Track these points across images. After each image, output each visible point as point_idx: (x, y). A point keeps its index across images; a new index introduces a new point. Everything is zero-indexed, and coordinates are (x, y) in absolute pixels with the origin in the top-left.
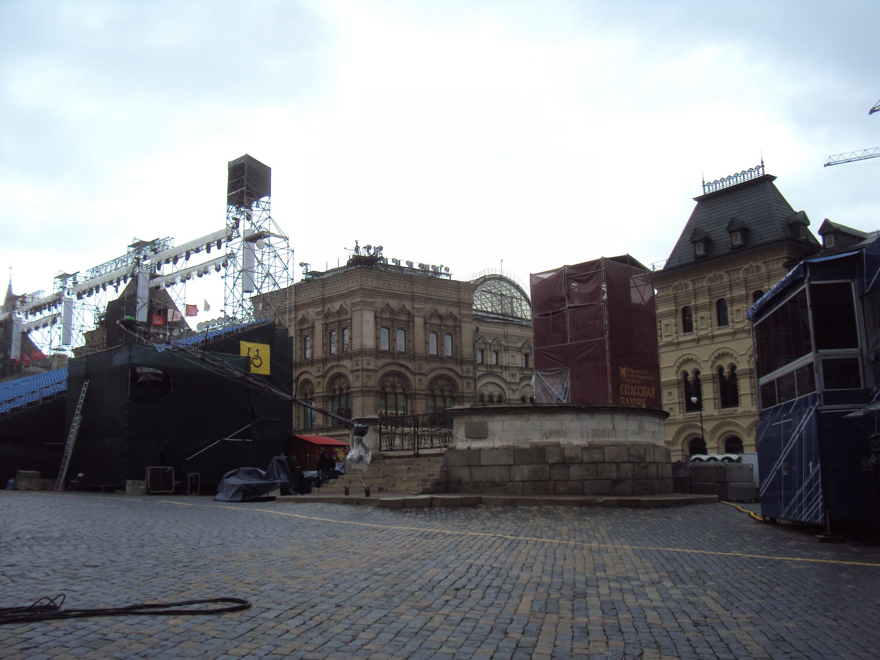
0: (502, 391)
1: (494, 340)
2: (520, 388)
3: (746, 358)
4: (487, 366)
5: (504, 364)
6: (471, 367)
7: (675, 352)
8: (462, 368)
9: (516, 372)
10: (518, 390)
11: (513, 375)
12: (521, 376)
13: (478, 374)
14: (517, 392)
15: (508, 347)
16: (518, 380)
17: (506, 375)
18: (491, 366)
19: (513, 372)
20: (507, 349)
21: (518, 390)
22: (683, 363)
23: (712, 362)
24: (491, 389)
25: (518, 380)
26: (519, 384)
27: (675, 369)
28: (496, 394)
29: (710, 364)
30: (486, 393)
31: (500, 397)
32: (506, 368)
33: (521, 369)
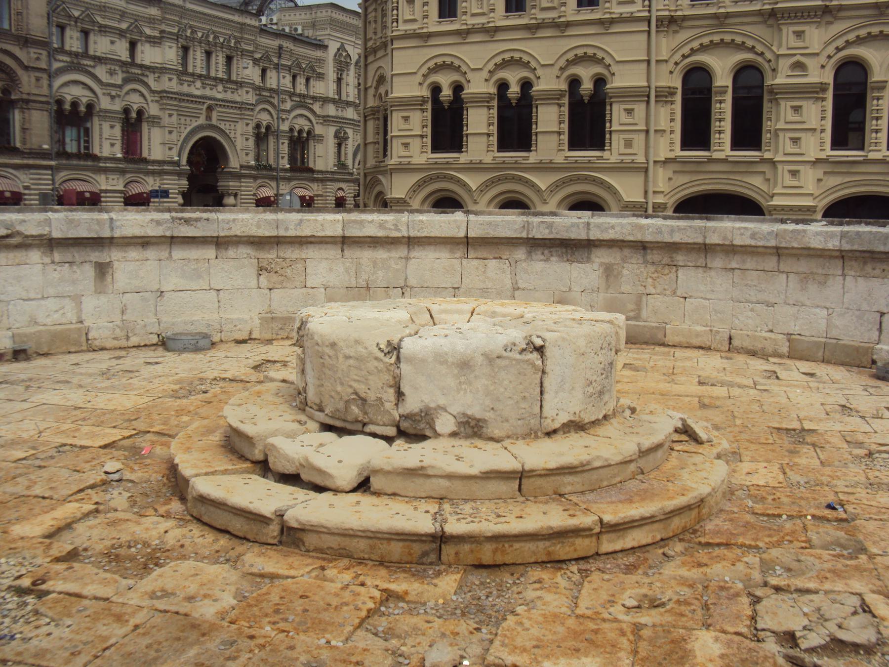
0: (92, 95)
1: (83, 12)
2: (122, 94)
3: (555, 71)
4: (70, 53)
5: (98, 54)
6: (45, 53)
7: (420, 49)
8: (28, 53)
9: (117, 68)
10: (119, 96)
11: (112, 73)
12: (125, 75)
13: (56, 65)
14: (117, 100)
15: (106, 26)
16: (119, 82)
17: (101, 72)
18: (76, 55)
19: (113, 67)
20: (103, 30)
21: (119, 96)
22: (434, 69)
23: (423, 75)
24: (76, 92)
25: (119, 82)
26: (120, 87)
27: (419, 78)
28: (84, 100)
29: (485, 74)
30: (69, 98)
31: (90, 106)
32: (99, 60)
33: (123, 64)
